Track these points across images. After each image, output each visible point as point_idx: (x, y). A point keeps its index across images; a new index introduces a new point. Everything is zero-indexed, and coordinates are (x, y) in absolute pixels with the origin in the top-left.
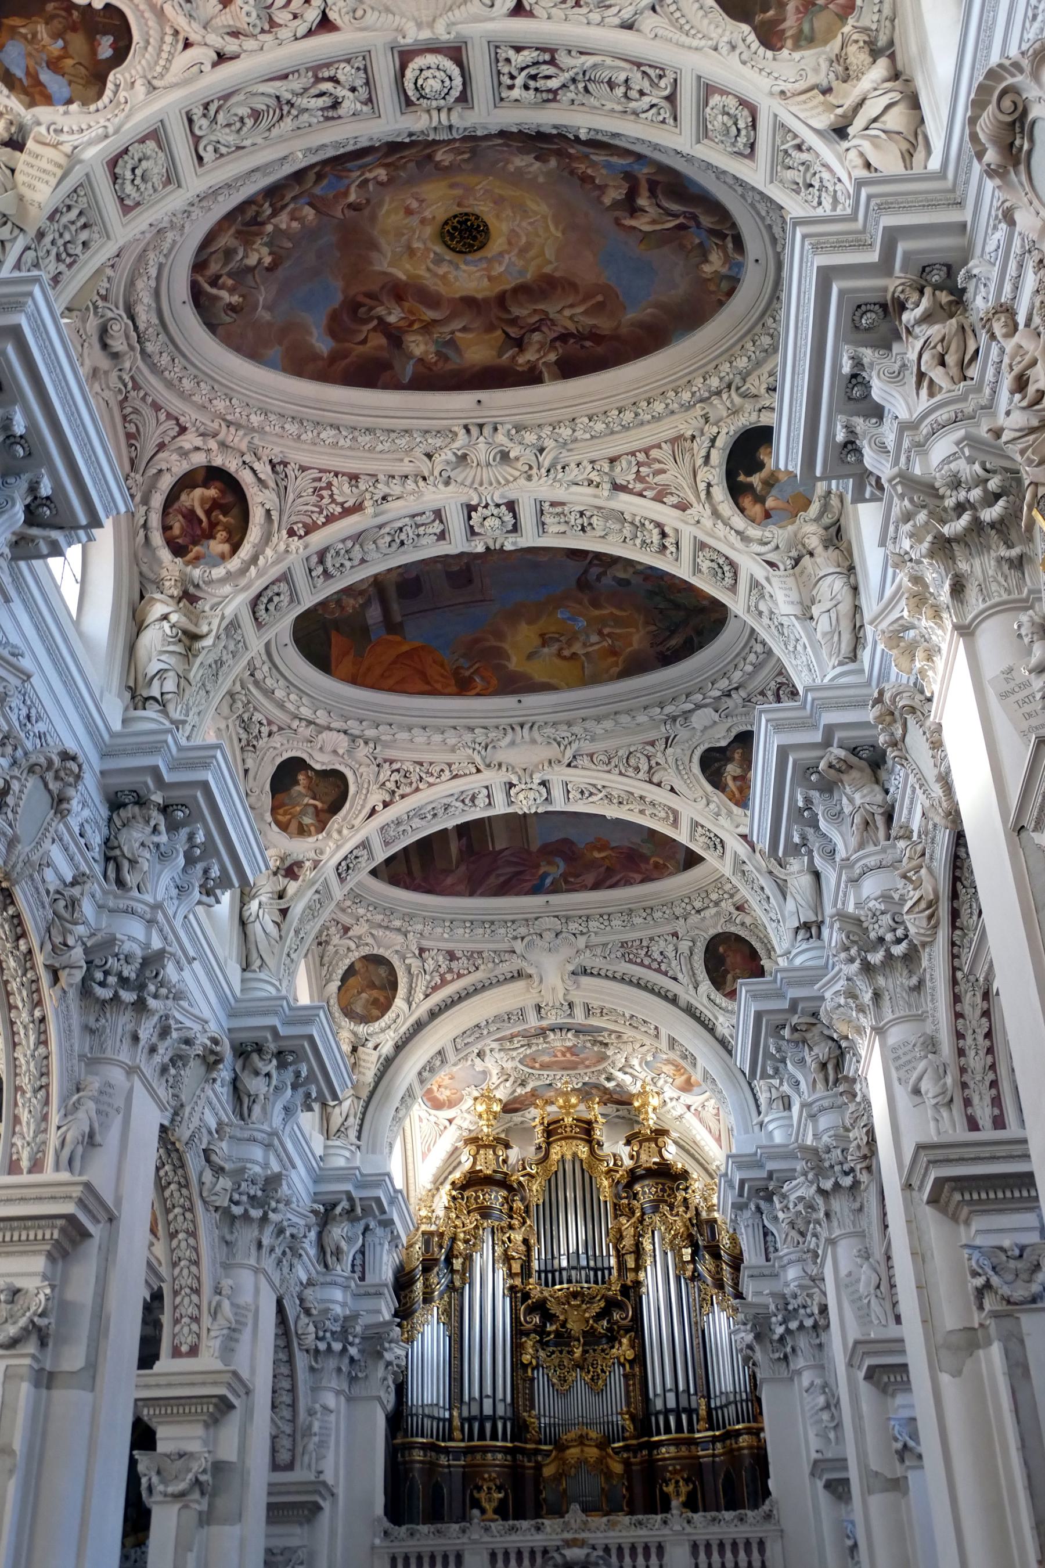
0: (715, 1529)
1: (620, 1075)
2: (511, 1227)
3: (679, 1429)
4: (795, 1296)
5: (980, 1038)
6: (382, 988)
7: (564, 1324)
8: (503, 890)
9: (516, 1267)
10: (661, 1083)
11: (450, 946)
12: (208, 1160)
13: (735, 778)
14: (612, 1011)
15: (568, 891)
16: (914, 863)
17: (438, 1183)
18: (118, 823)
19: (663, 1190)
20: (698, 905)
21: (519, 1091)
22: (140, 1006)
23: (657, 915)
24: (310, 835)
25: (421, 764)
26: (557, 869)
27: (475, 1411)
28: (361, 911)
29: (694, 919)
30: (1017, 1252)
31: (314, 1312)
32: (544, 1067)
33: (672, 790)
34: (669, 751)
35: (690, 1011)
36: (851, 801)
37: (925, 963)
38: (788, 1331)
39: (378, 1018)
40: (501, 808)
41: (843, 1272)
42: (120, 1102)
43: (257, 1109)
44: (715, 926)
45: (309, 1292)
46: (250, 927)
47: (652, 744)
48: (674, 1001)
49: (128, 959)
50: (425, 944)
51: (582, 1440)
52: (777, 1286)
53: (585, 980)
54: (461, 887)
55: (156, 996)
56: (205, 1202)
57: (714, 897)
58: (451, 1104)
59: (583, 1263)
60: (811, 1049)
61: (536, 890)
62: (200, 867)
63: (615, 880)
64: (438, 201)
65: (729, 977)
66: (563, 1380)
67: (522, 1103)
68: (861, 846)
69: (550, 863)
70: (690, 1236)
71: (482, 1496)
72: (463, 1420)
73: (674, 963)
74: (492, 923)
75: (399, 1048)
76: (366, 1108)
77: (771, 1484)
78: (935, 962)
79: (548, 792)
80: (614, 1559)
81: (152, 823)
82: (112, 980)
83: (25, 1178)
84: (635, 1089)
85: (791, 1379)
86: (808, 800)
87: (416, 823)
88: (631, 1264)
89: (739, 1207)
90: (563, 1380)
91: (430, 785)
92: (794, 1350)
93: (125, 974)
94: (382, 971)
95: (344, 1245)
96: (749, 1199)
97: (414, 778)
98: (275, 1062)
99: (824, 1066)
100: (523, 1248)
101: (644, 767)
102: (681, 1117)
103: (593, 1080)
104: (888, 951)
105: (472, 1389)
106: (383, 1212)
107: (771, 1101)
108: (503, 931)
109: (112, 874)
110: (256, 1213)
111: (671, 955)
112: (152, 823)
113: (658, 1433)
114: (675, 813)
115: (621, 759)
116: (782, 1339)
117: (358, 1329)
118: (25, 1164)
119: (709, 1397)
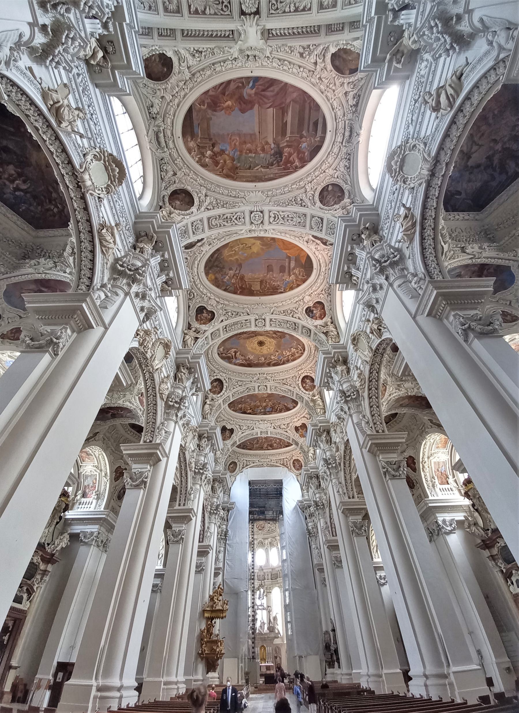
8: (272, 82)
15: (242, 78)
26: (248, 91)
28: (335, 104)
61: (257, 79)
63: (221, 88)
64: (265, 350)
65: (158, 60)
69: (250, 95)
73: (188, 55)
94: (337, 63)
111: (190, 58)
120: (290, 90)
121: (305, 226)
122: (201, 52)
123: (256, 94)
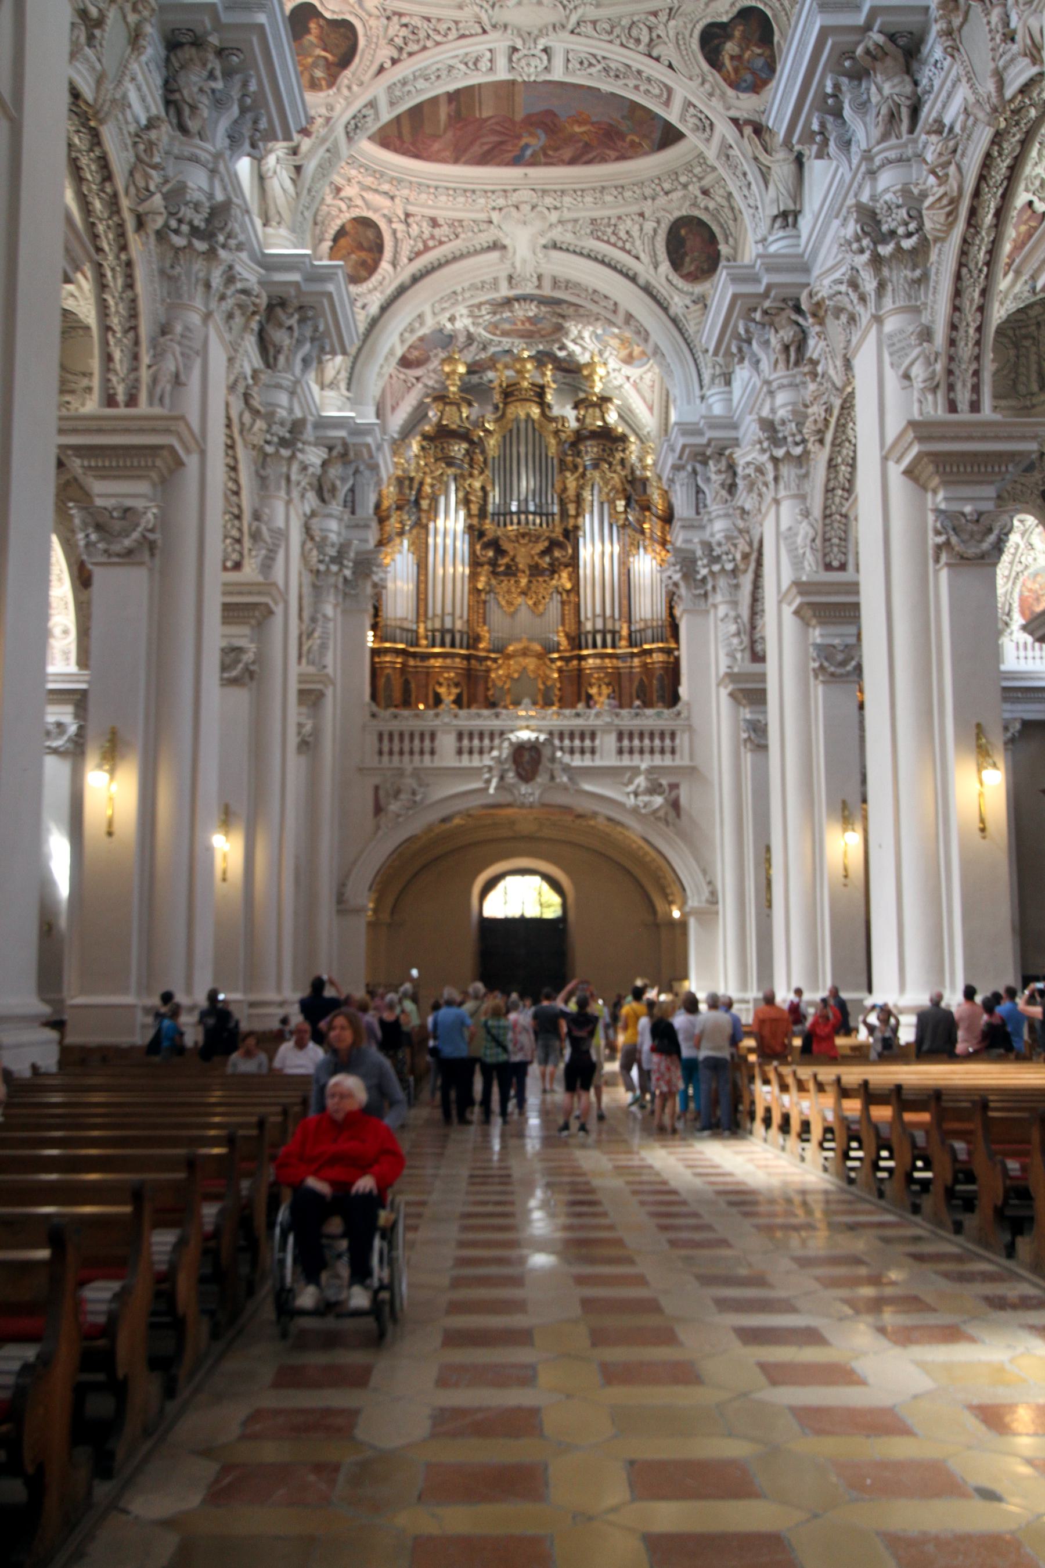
0: (637, 722)
1: (571, 346)
2: (471, 475)
3: (604, 646)
4: (719, 544)
5: (971, 331)
6: (370, 250)
7: (513, 559)
8: (483, 160)
9: (475, 509)
10: (606, 354)
11: (432, 213)
12: (247, 403)
13: (732, 58)
14: (577, 285)
15: (547, 164)
16: (944, 159)
17: (406, 432)
18: (177, 65)
19: (604, 450)
20: (667, 186)
21: (483, 355)
22: (211, 254)
23: (628, 194)
24: (321, 89)
25: (429, 20)
26: (536, 141)
27: (438, 625)
28: (353, 172)
29: (662, 200)
30: (975, 517)
31: (317, 539)
32: (505, 334)
33: (670, 66)
34: (672, 23)
35: (648, 290)
36: (880, 90)
37: (933, 257)
38: (712, 573)
39: (365, 279)
40: (502, 74)
41: (784, 525)
42: (197, 345)
43: (282, 359)
44: (679, 209)
45: (315, 523)
46: (268, 182)
47: (655, 14)
48: (633, 279)
49: (197, 206)
50: (411, 209)
51: (525, 653)
52: (706, 536)
53: (555, 254)
54: (448, 153)
55: (224, 246)
56: (244, 440)
57: (683, 179)
58: (418, 363)
59: (532, 508)
60: (777, 331)
61: (517, 161)
62: (249, 116)
63: (591, 156)
65: (688, 259)
66: (510, 603)
67: (480, 366)
68: (885, 137)
69: (531, 134)
70: (625, 490)
71: (442, 690)
72: (426, 630)
73: (638, 243)
74: (474, 192)
75: (384, 309)
76: (354, 363)
77: (683, 691)
78: (944, 260)
79: (549, 60)
80: (557, 742)
81: (209, 66)
82: (185, 228)
83: (122, 411)
84: (584, 359)
85: (707, 612)
86: (837, 86)
87: (421, 84)
88: (572, 511)
89: (677, 468)
90: (510, 603)
91: (438, 44)
92: (714, 588)
93: (196, 223)
94: (370, 234)
95: (338, 483)
96: (687, 461)
97: (422, 35)
98: (296, 317)
99: (786, 348)
100: (480, 494)
101: (645, 39)
102: (621, 386)
103: (547, 349)
104: (898, 244)
105: (435, 605)
106: (371, 457)
107: (713, 377)
108: (482, 201)
109: (175, 121)
110: (285, 453)
111: (635, 233)
112: (209, 66)
113: (587, 648)
114: (670, 91)
115: (623, 28)
116: (704, 580)
117: (352, 555)
118: (121, 398)
119: (630, 622)
120: (448, 153)
121: (389, 88)
122: (614, 233)
123: (519, 137)
